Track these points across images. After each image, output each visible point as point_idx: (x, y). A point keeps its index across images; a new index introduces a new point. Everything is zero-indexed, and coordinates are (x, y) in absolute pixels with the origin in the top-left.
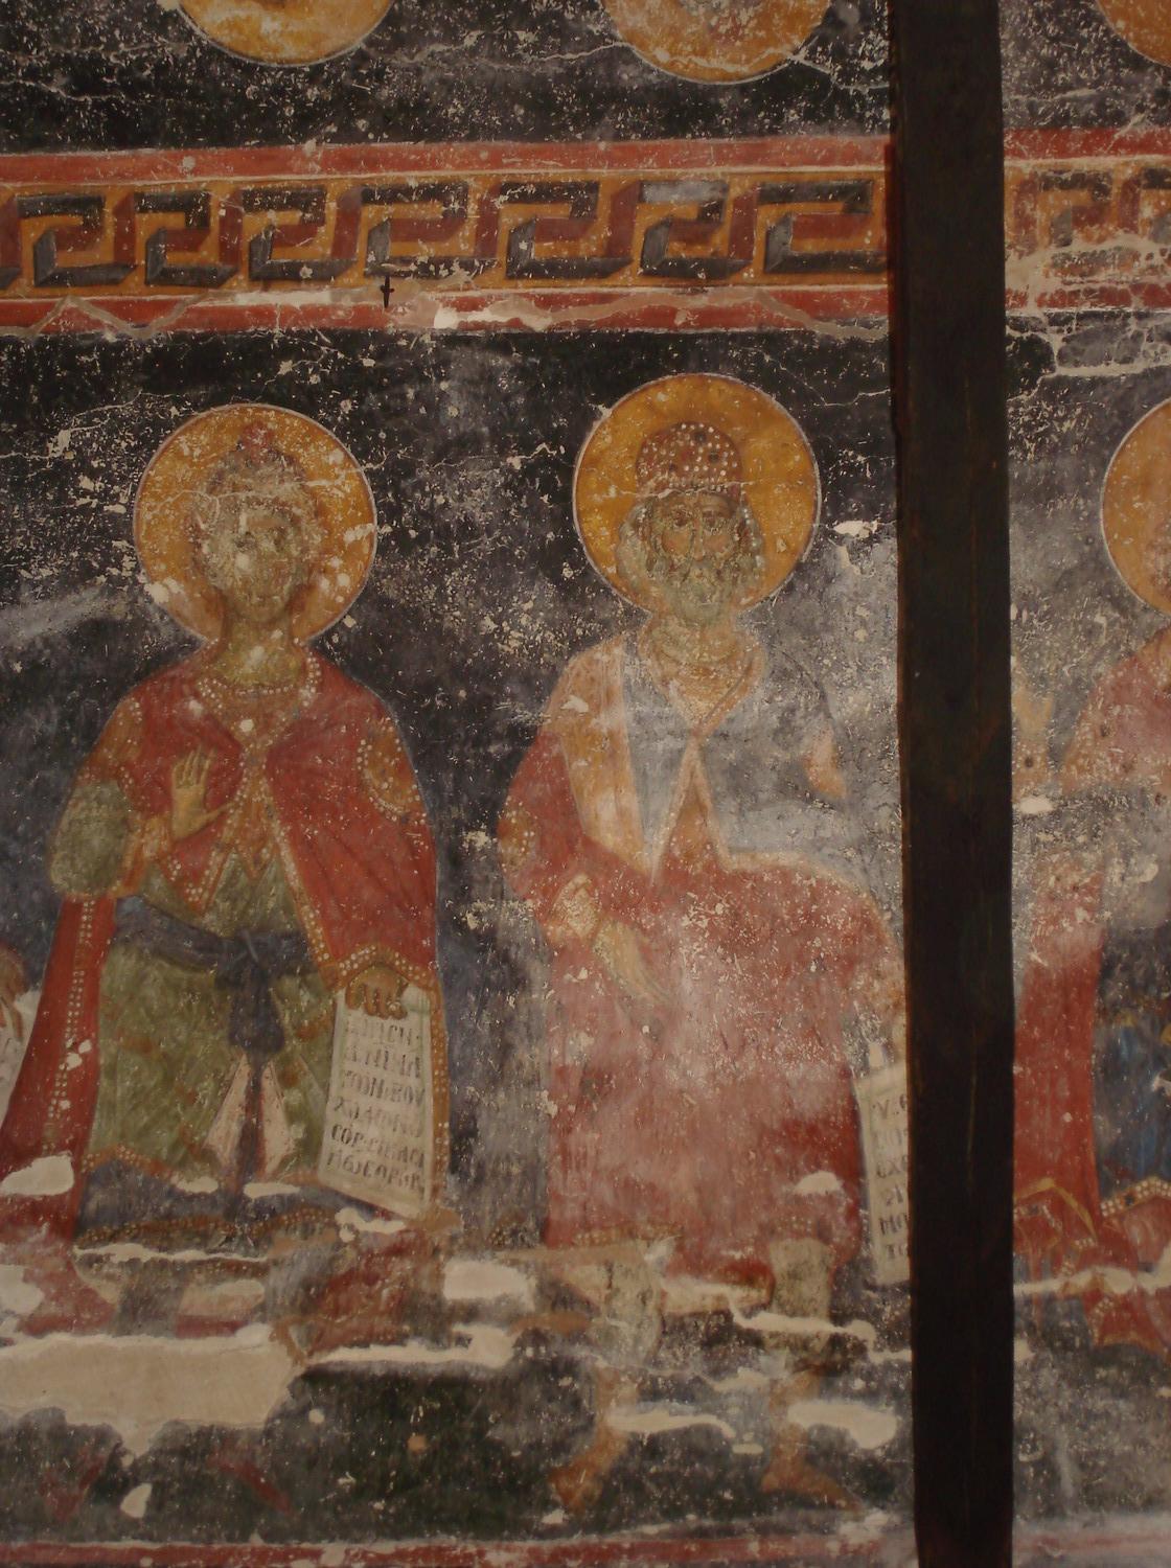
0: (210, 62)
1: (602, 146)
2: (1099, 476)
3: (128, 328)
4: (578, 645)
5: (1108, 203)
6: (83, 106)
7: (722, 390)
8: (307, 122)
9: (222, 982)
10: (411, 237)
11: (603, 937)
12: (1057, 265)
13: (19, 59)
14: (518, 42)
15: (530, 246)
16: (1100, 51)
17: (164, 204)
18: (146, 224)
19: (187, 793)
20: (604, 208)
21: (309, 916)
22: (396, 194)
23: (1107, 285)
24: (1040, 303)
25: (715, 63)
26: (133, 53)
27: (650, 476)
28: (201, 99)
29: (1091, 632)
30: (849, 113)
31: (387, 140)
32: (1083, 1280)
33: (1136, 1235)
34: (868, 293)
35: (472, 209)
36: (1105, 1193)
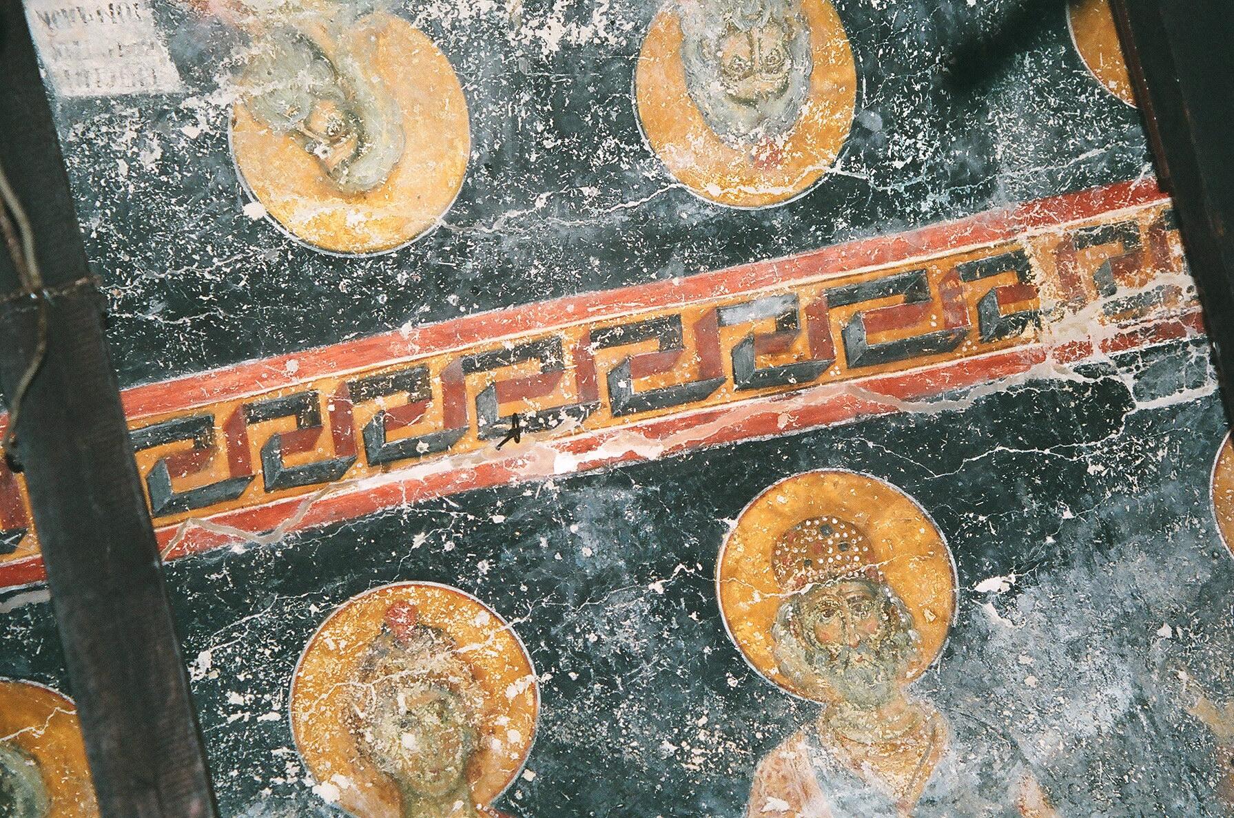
0: (302, 263)
1: (676, 281)
2: (1204, 494)
3: (254, 537)
4: (760, 749)
5: (1140, 249)
6: (182, 328)
7: (836, 485)
8: (400, 307)
10: (517, 397)
14: (584, 198)
15: (628, 384)
16: (1099, 112)
18: (258, 434)
20: (689, 338)
22: (493, 360)
23: (1158, 322)
24: (1104, 349)
25: (762, 190)
26: (227, 266)
27: (789, 574)
28: (298, 301)
30: (891, 212)
31: (479, 310)
34: (946, 369)
35: (568, 360)
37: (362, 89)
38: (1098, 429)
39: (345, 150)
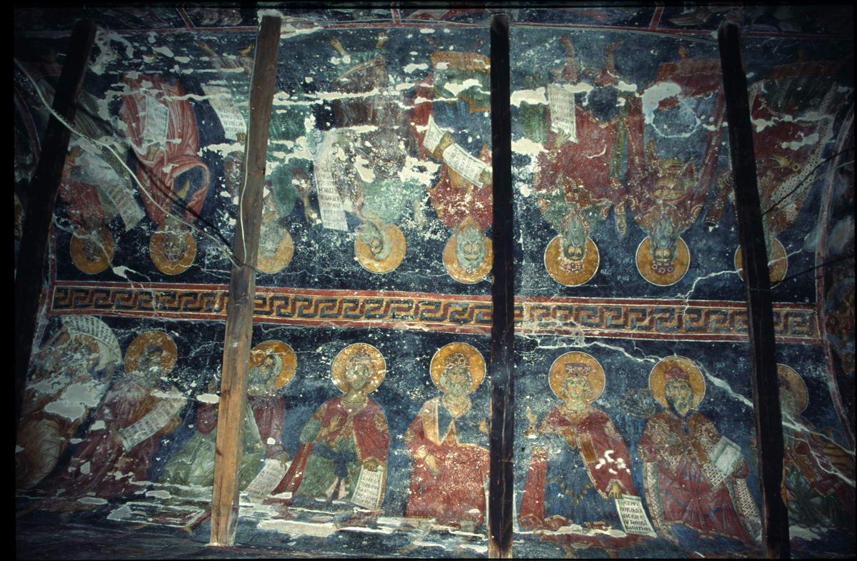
3: (338, 326)
4: (428, 398)
7: (465, 346)
8: (381, 286)
9: (335, 462)
11: (427, 458)
12: (539, 325)
13: (325, 270)
17: (349, 301)
19: (334, 424)
21: (358, 450)
22: (398, 302)
29: (546, 402)
32: (539, 532)
33: (553, 525)
35: (414, 306)
36: (546, 517)
37: (384, 239)
38: (528, 350)
39: (378, 250)
